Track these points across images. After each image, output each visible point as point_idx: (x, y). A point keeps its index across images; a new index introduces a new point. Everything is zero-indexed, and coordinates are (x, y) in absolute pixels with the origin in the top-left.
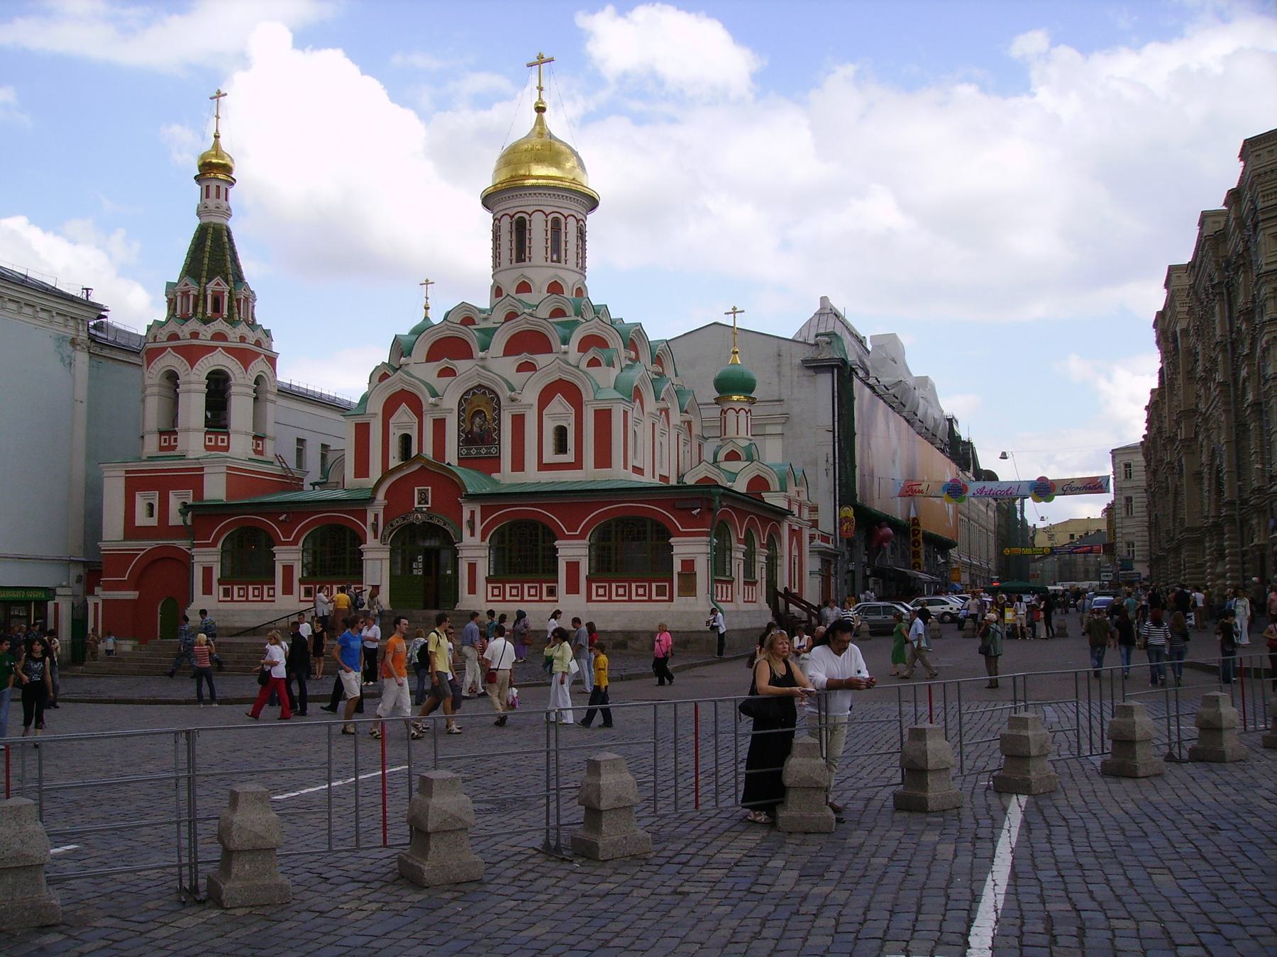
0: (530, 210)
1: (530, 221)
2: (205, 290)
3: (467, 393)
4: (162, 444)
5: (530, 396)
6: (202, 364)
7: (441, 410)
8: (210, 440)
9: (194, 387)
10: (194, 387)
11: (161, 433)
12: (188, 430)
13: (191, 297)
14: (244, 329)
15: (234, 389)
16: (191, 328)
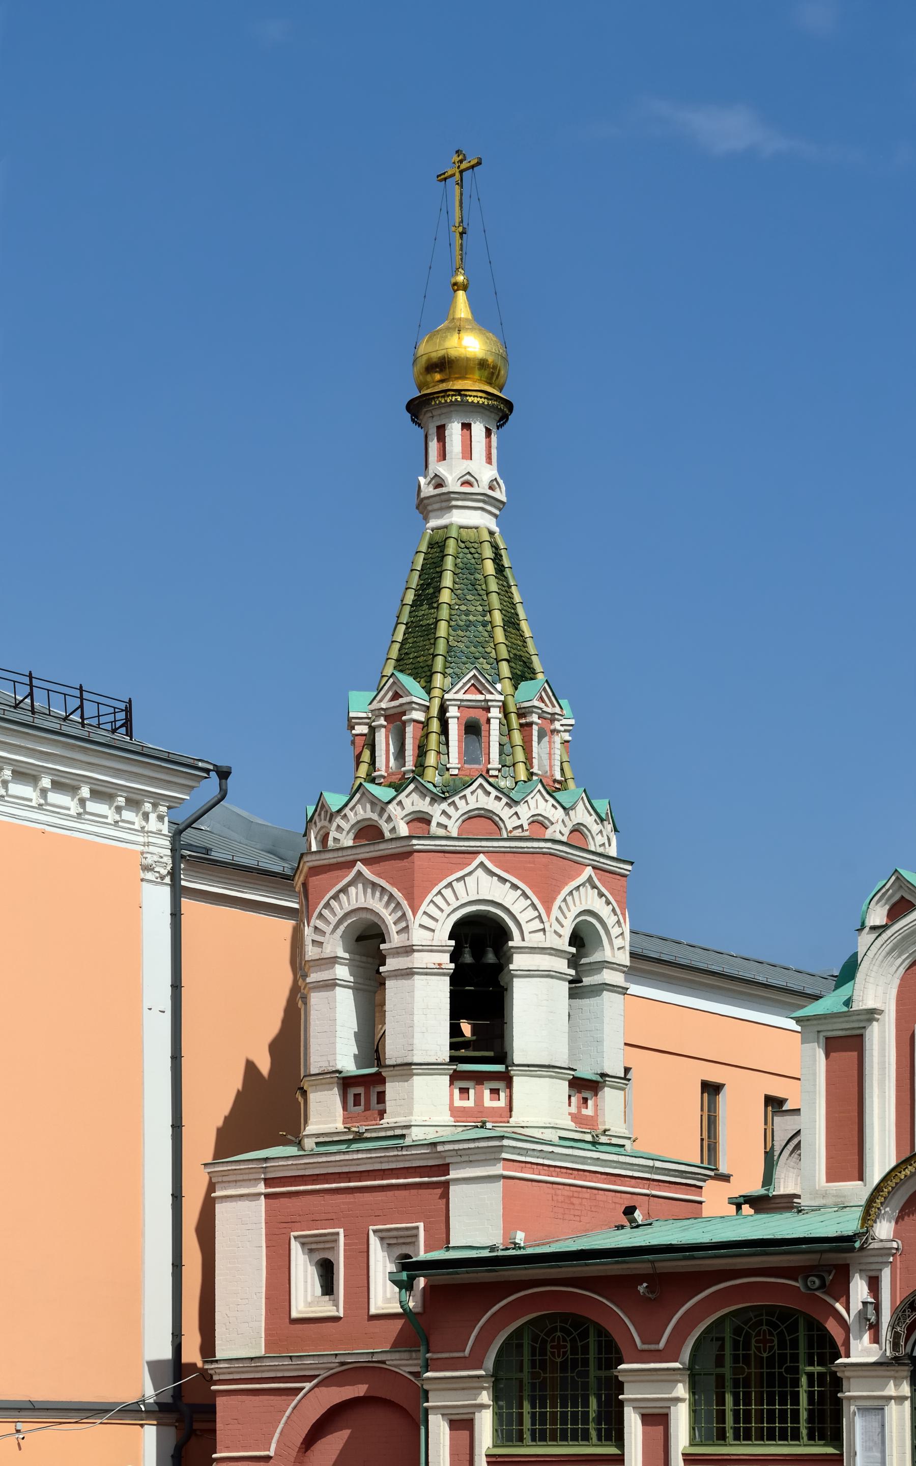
2: (443, 709)
6: (439, 900)
9: (420, 960)
10: (420, 960)
11: (346, 1083)
12: (407, 1069)
13: (409, 730)
15: (519, 962)
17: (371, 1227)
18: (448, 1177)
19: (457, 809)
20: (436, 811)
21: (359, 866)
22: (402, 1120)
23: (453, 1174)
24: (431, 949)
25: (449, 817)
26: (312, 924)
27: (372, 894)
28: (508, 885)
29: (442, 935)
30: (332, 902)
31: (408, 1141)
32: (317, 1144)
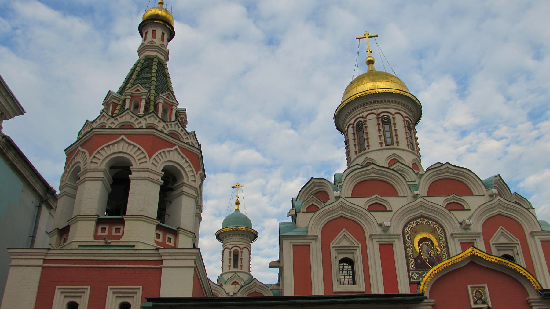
0: (393, 111)
1: (394, 118)
3: (408, 222)
4: (99, 234)
5: (477, 227)
6: (159, 156)
7: (390, 235)
8: (158, 236)
11: (100, 221)
14: (193, 138)
16: (149, 121)
17: (109, 287)
18: (162, 265)
19: (168, 127)
20: (161, 126)
21: (123, 136)
22: (133, 239)
23: (165, 263)
24: (155, 173)
25: (165, 129)
26: (93, 155)
27: (128, 148)
28: (184, 160)
29: (159, 168)
30: (105, 148)
31: (136, 248)
32: (79, 246)
